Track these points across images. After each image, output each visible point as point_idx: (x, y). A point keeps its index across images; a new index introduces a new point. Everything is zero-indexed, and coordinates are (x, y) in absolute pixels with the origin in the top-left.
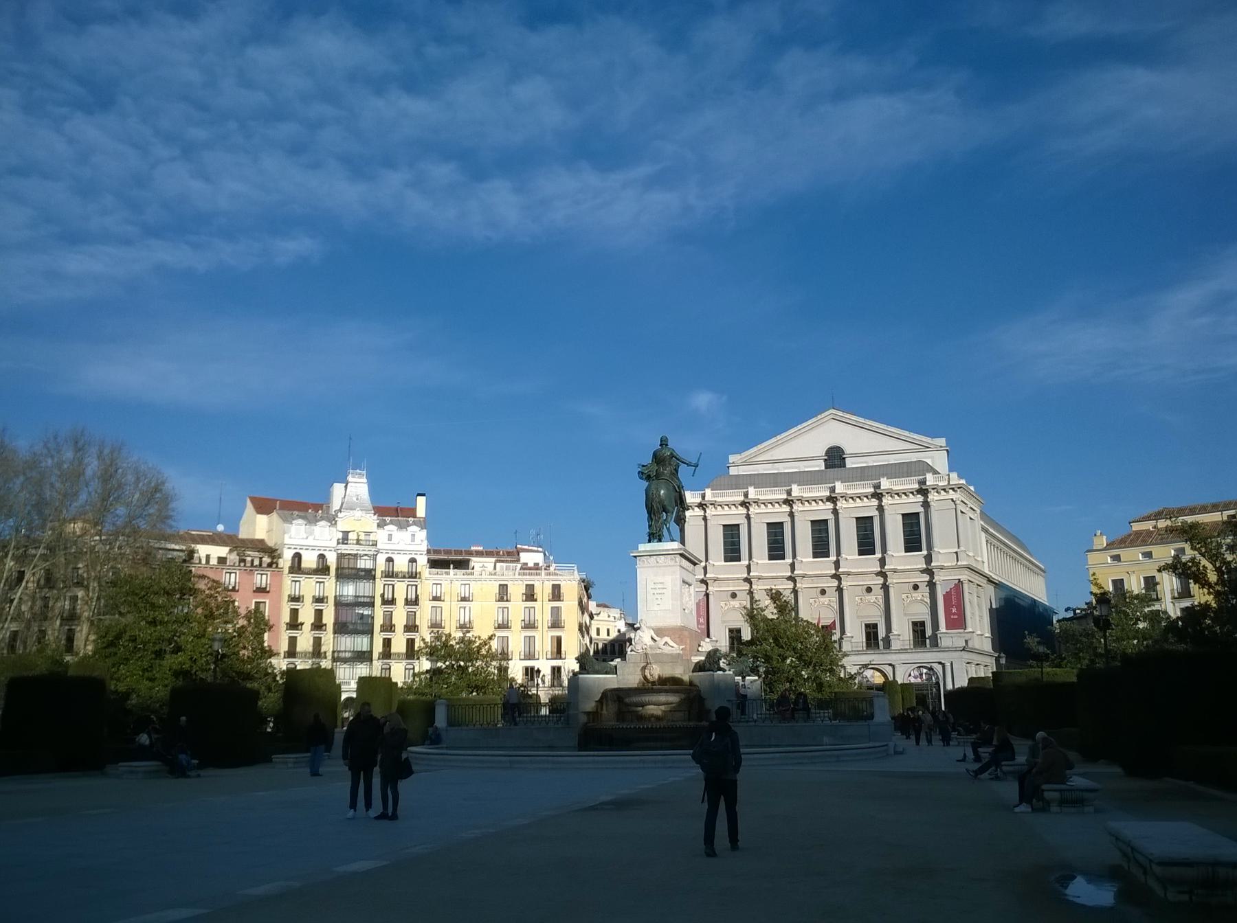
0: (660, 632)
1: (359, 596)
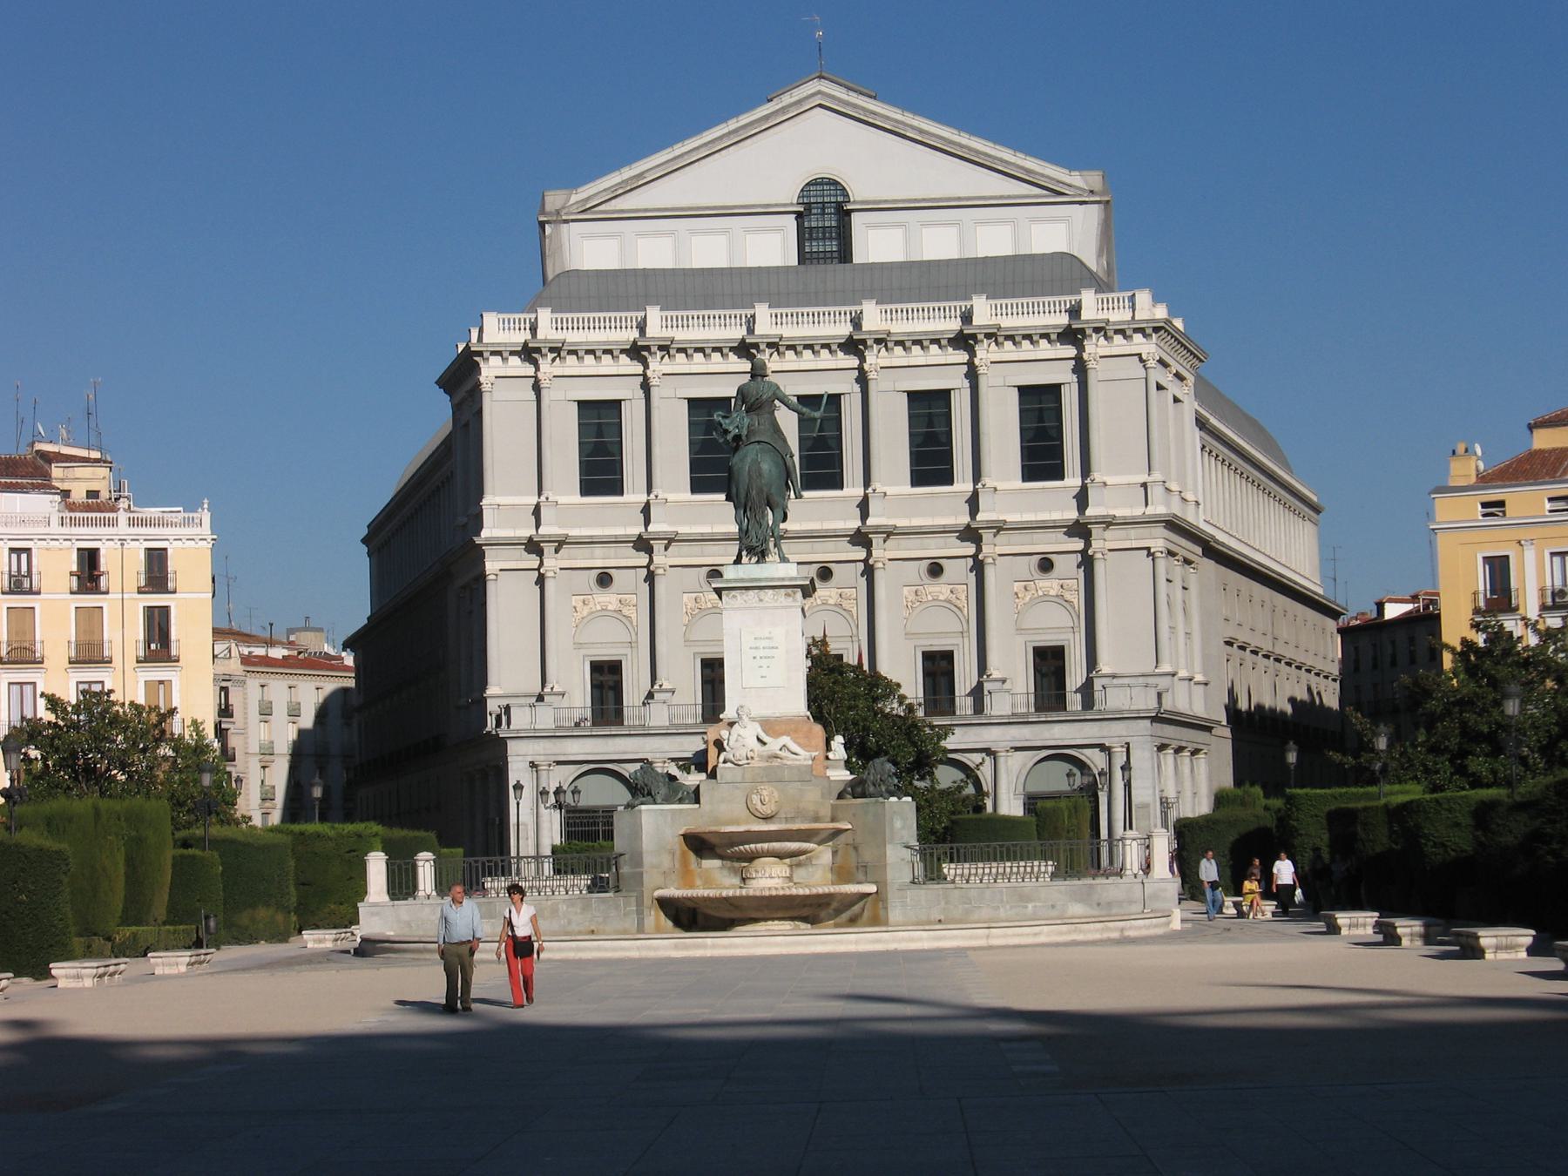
0: (771, 726)
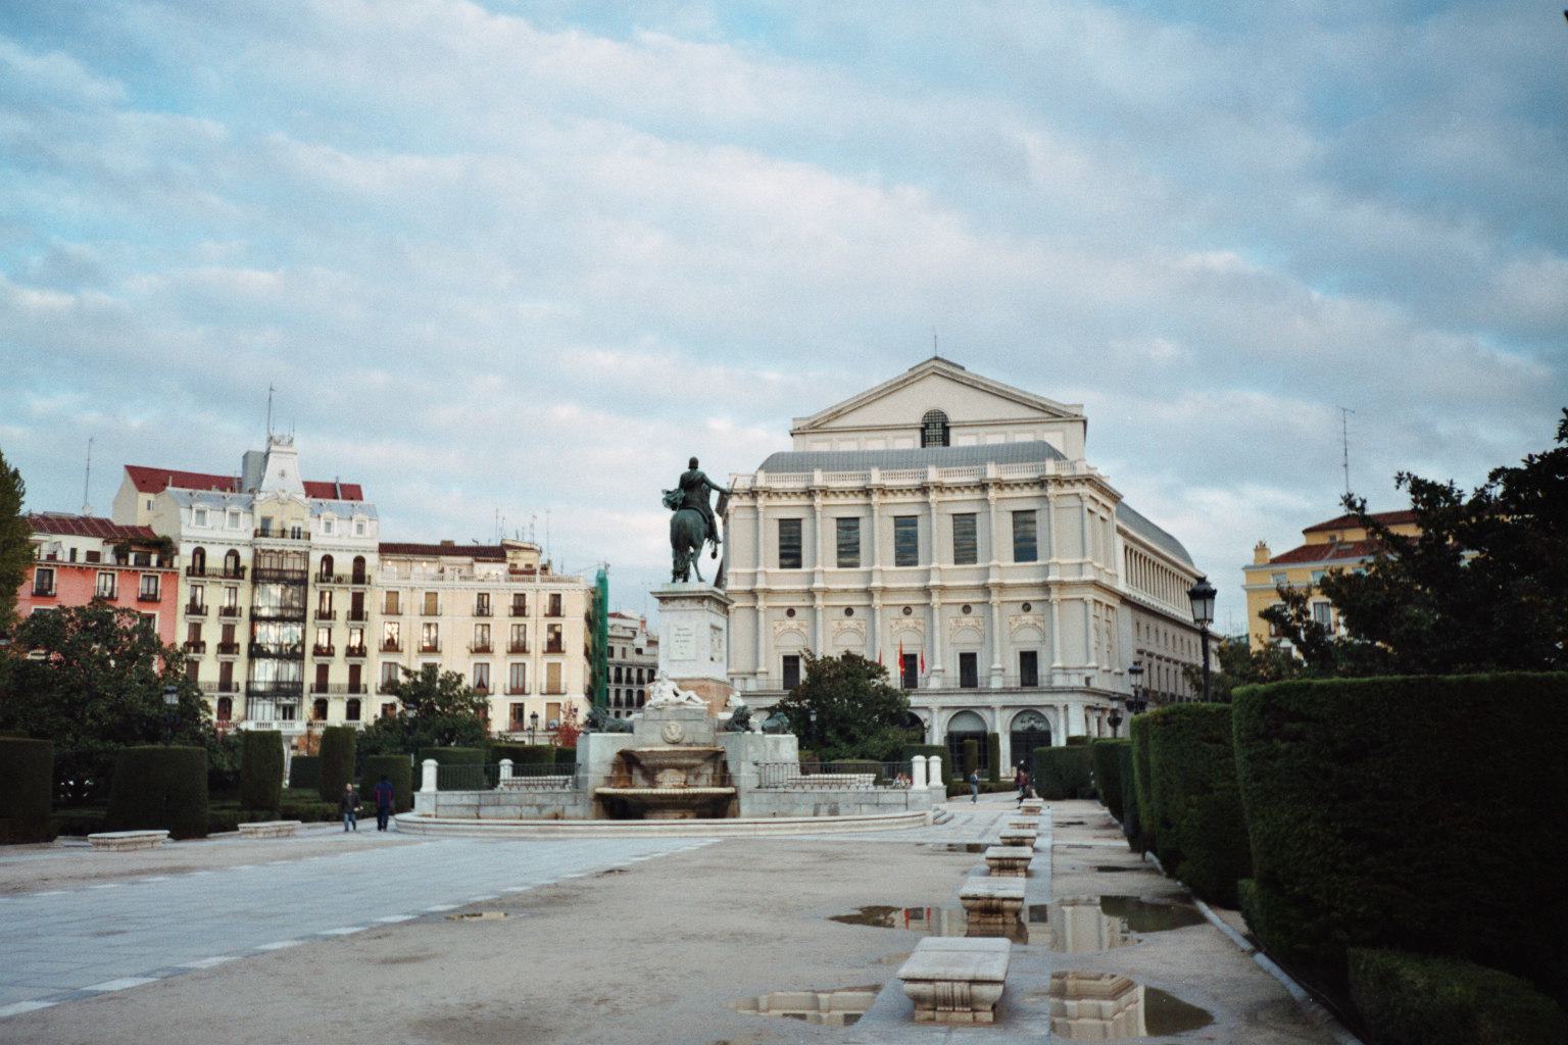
0: (682, 683)
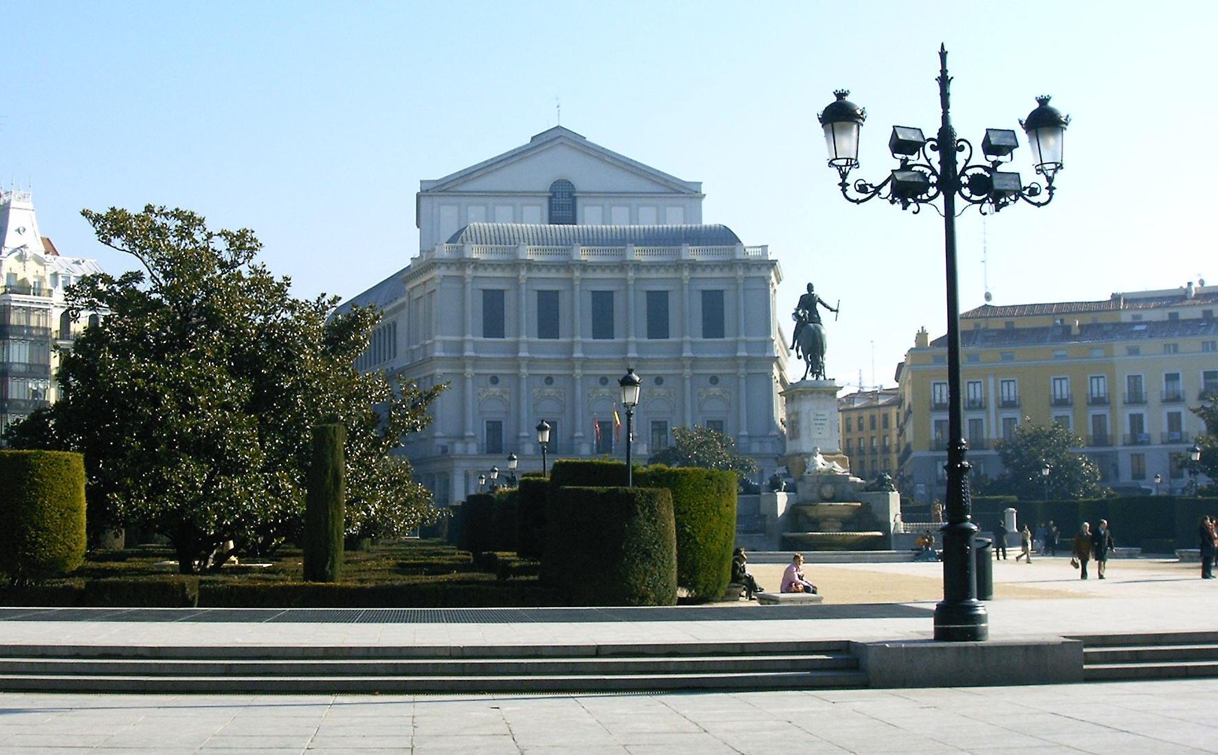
1: (33, 365)
